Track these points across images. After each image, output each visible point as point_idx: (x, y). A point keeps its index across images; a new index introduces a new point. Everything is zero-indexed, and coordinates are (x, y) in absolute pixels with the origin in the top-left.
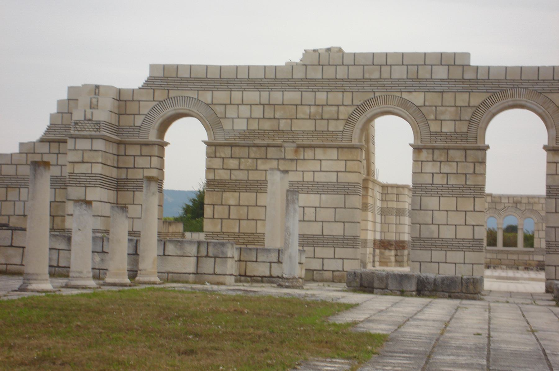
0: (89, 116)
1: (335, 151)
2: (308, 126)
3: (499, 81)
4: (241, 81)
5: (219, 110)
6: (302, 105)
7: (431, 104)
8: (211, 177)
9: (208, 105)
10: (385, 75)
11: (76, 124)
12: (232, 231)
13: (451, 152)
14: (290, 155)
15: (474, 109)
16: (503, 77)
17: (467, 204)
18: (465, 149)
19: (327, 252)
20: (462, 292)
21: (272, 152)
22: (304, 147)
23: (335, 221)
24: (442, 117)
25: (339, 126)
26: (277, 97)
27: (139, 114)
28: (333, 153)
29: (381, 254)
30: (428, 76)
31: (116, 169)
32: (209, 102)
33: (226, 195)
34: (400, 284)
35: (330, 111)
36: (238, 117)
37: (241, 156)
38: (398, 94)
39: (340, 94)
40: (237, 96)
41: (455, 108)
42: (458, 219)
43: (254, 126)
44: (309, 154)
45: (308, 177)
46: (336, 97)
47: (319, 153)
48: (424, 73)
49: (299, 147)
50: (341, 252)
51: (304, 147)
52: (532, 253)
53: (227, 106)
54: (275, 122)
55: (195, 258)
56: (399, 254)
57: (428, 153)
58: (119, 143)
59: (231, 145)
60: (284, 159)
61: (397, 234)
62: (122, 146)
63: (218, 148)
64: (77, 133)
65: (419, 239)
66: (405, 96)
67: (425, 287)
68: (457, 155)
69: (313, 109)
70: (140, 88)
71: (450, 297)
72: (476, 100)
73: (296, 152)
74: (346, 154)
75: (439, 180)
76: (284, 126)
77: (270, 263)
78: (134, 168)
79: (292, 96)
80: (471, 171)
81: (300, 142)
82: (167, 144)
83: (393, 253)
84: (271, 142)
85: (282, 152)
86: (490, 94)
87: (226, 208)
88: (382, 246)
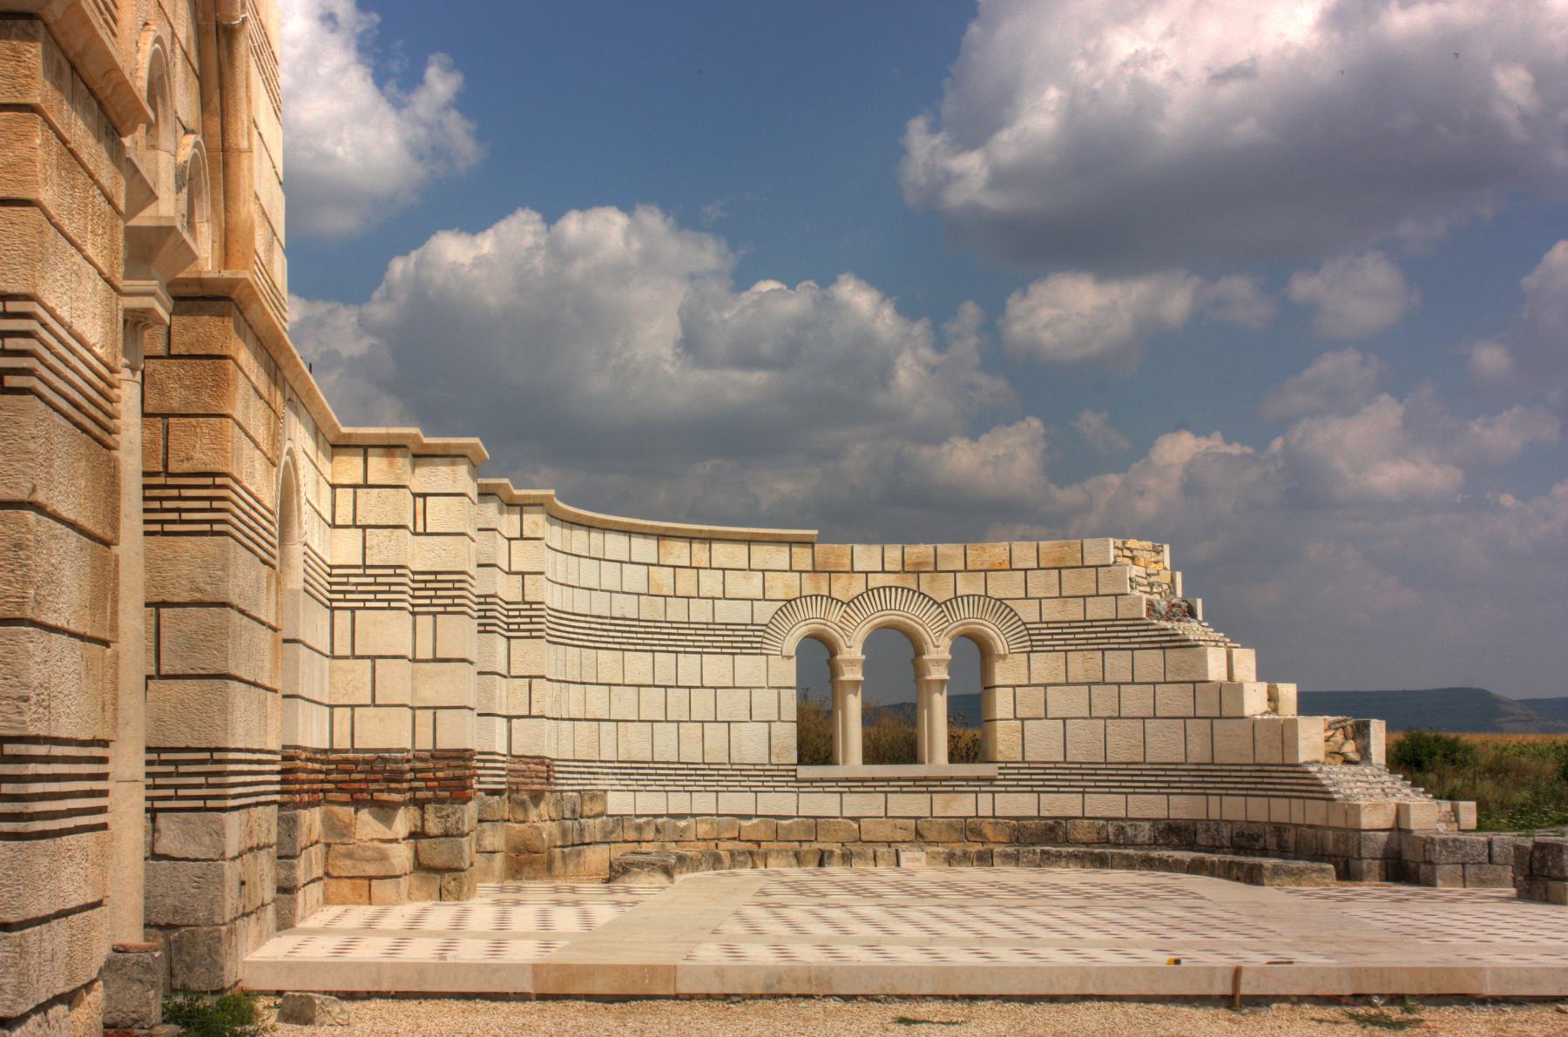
56: (433, 826)
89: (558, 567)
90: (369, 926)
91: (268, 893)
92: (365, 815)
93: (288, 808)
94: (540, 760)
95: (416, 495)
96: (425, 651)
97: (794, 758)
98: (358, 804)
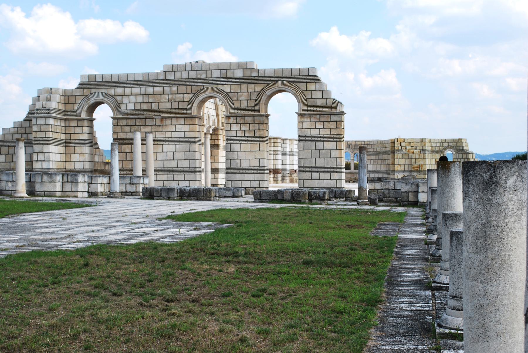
0: (44, 106)
1: (183, 119)
2: (168, 106)
3: (270, 77)
4: (130, 81)
5: (119, 98)
6: (164, 94)
7: (234, 91)
8: (116, 137)
9: (112, 96)
10: (209, 76)
11: (37, 110)
12: (128, 167)
13: (246, 118)
14: (158, 123)
15: (258, 93)
16: (273, 75)
17: (256, 147)
18: (254, 116)
19: (181, 177)
20: (203, 196)
21: (148, 122)
22: (166, 118)
23: (184, 160)
24: (240, 99)
25: (185, 105)
26: (150, 90)
27: (76, 103)
28: (182, 121)
30: (232, 76)
31: (64, 135)
32: (113, 94)
33: (124, 147)
34: (168, 193)
35: (179, 97)
36: (129, 103)
37: (132, 124)
38: (216, 86)
39: (184, 88)
40: (128, 91)
41: (247, 93)
42: (251, 155)
43: (138, 107)
44: (169, 122)
45: (169, 135)
46: (182, 89)
47: (174, 121)
48: (230, 74)
49: (163, 118)
50: (188, 177)
51: (166, 118)
53: (123, 96)
54: (149, 104)
55: (61, 183)
56: (275, 176)
57: (233, 119)
58: (65, 120)
59: (126, 119)
60: (155, 125)
61: (274, 165)
62: (67, 122)
63: (118, 120)
64: (38, 115)
65: (230, 167)
66: (220, 87)
67: (184, 194)
68: (249, 119)
69: (170, 96)
70: (75, 89)
71: (197, 200)
72: (258, 88)
73: (162, 121)
74: (189, 121)
75: (240, 134)
76: (154, 106)
77: (126, 184)
78: (74, 133)
79: (158, 89)
80: (258, 128)
81: (163, 115)
82: (94, 119)
84: (147, 116)
85: (154, 121)
86: (266, 85)
87: (125, 154)
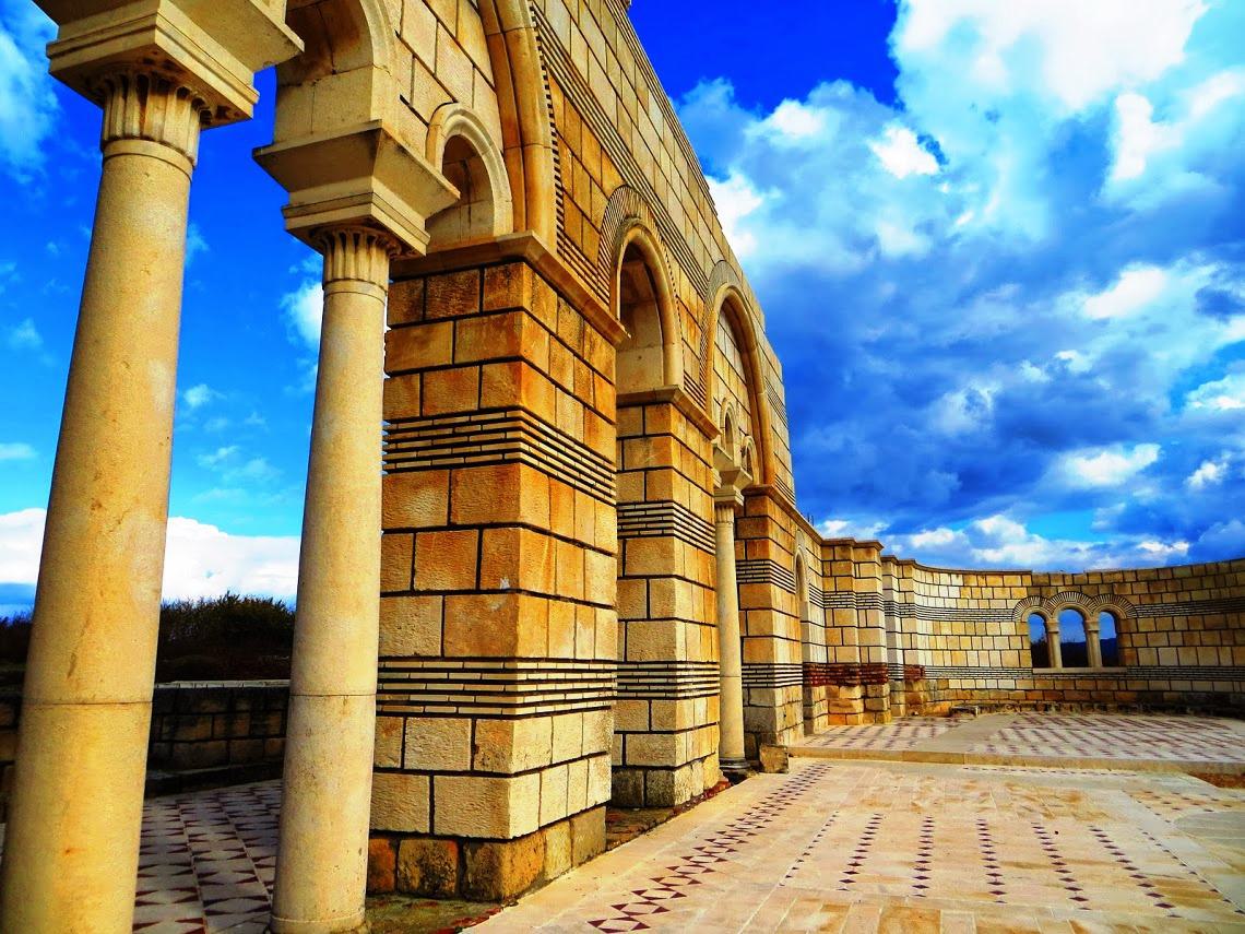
29: (831, 696)
52: (1125, 677)
56: (871, 693)
61: (865, 650)
83: (857, 692)
88: (832, 678)
89: (922, 589)
90: (842, 734)
91: (800, 719)
92: (843, 689)
93: (807, 688)
94: (917, 667)
95: (855, 563)
96: (863, 624)
97: (1030, 665)
98: (840, 685)
